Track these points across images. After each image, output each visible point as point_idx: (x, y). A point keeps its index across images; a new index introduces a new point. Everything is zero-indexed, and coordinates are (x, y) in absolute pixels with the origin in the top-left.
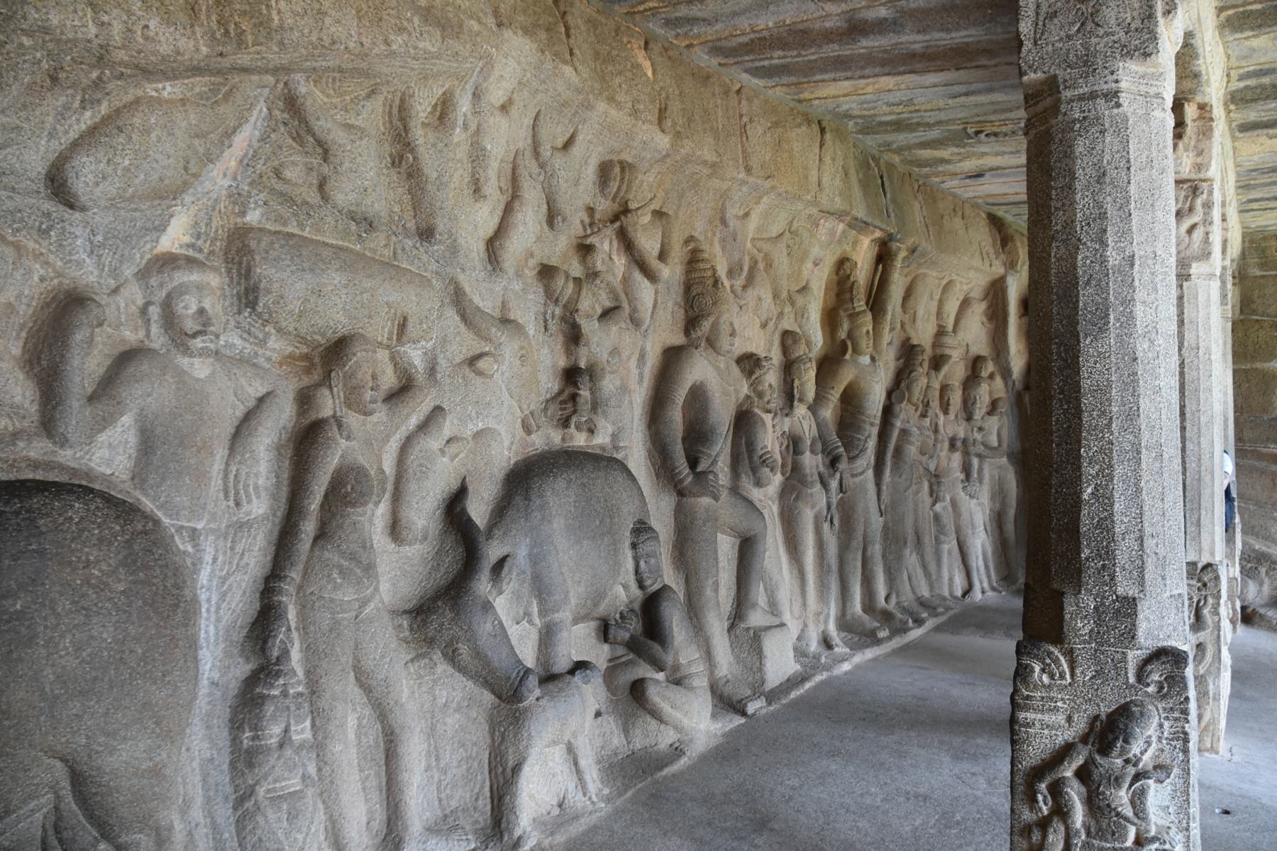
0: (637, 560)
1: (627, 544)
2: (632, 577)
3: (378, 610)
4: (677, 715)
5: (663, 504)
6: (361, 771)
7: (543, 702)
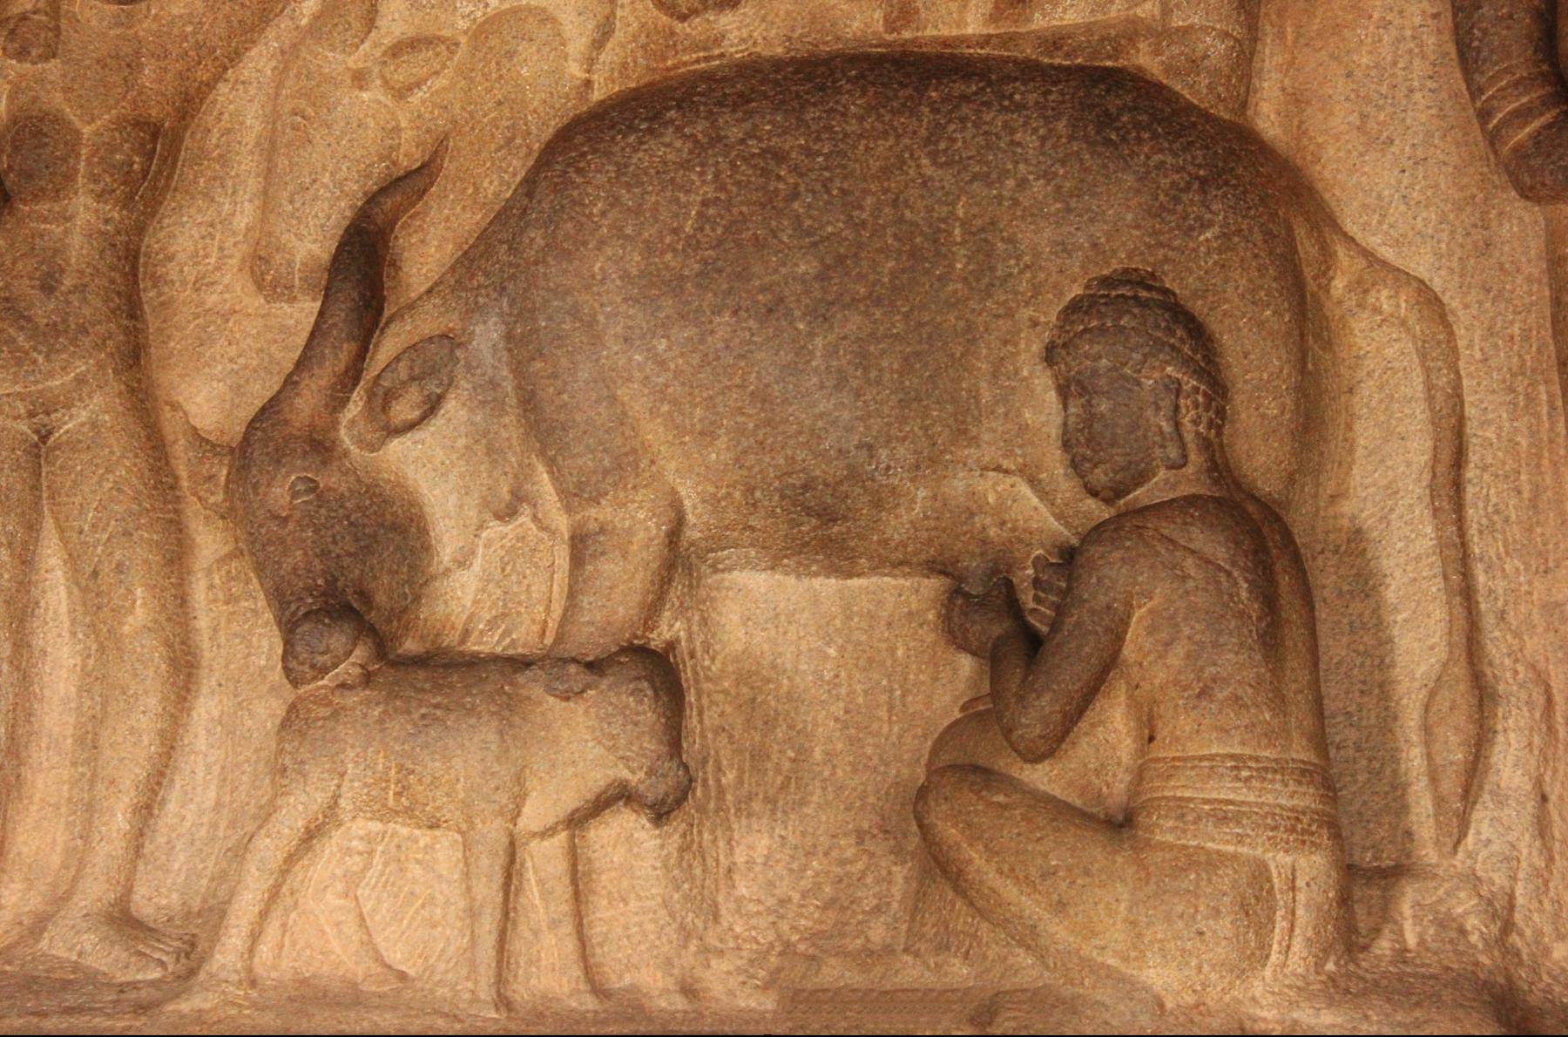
0: (1064, 393)
1: (1031, 347)
2: (1055, 465)
3: (94, 425)
4: (1030, 906)
5: (1507, 230)
6: (74, 764)
7: (352, 699)
